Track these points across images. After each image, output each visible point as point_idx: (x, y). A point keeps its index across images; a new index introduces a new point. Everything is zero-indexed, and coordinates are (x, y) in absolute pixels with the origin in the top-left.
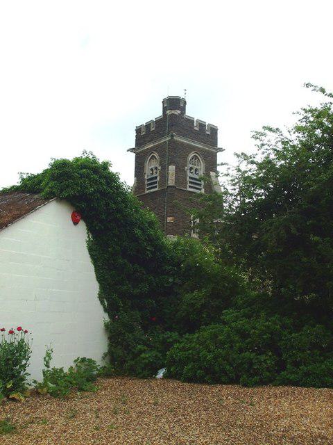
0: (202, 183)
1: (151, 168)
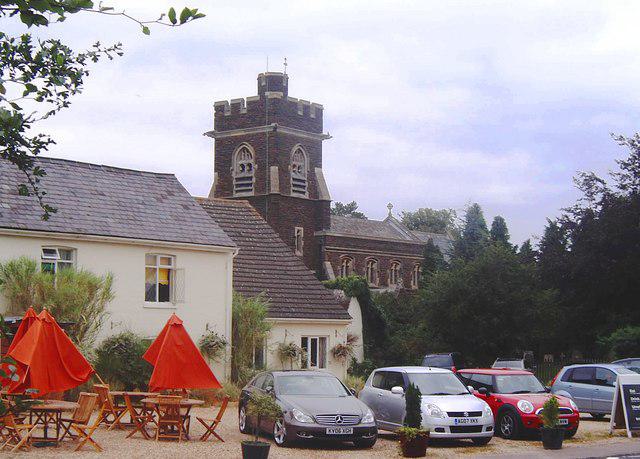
0: (306, 184)
1: (240, 163)
